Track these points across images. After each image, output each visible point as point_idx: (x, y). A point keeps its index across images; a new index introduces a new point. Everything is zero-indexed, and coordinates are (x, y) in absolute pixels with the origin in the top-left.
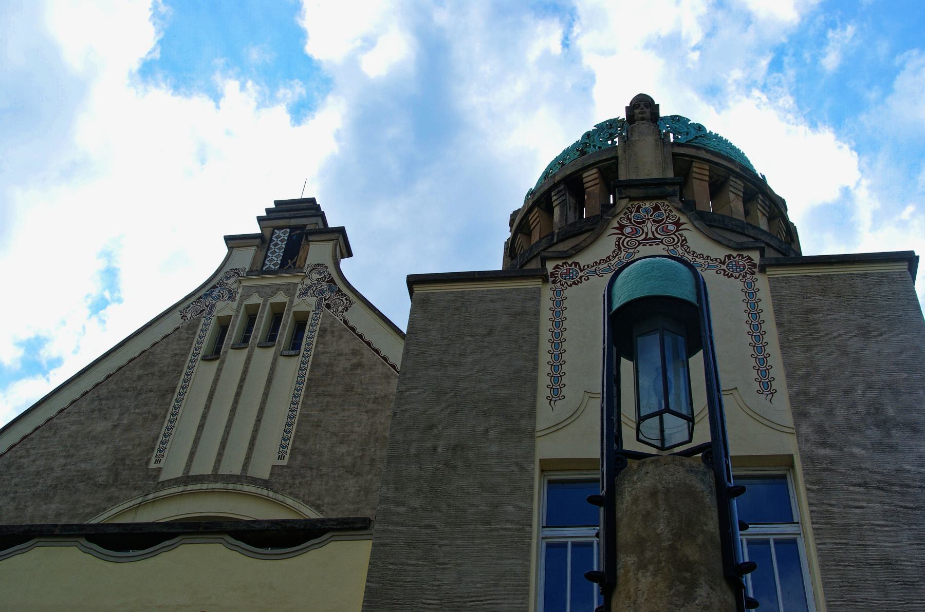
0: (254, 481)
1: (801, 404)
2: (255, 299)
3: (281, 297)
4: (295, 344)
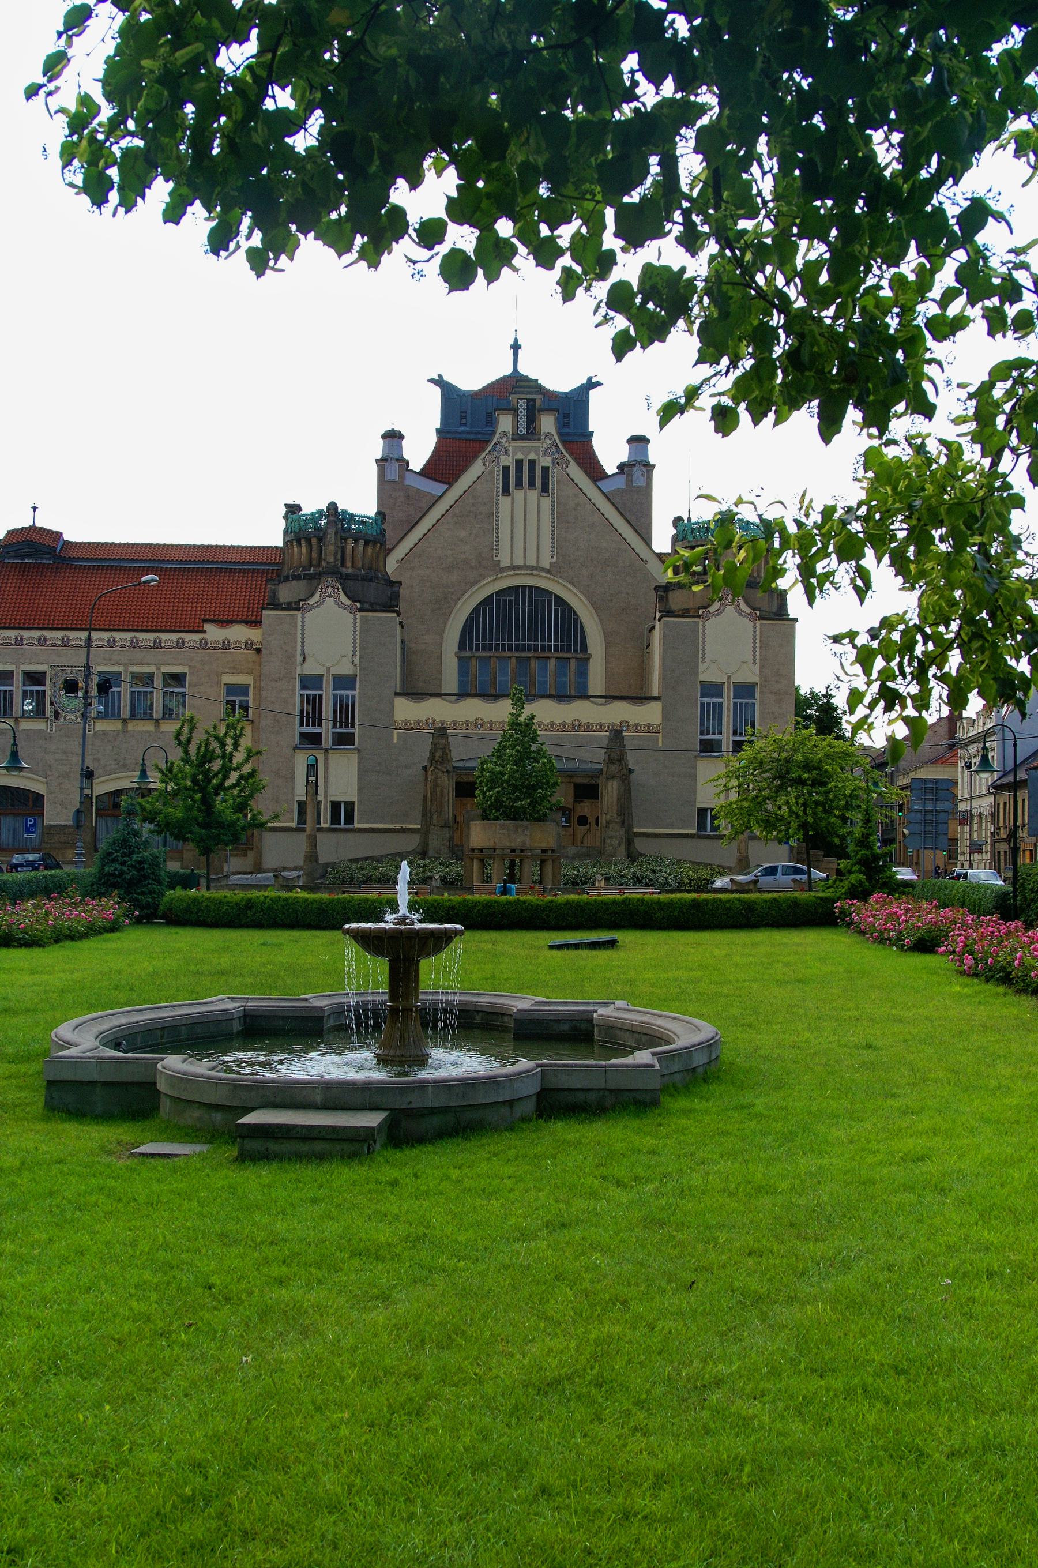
0: (543, 570)
1: (762, 667)
2: (519, 456)
3: (532, 456)
4: (545, 489)
